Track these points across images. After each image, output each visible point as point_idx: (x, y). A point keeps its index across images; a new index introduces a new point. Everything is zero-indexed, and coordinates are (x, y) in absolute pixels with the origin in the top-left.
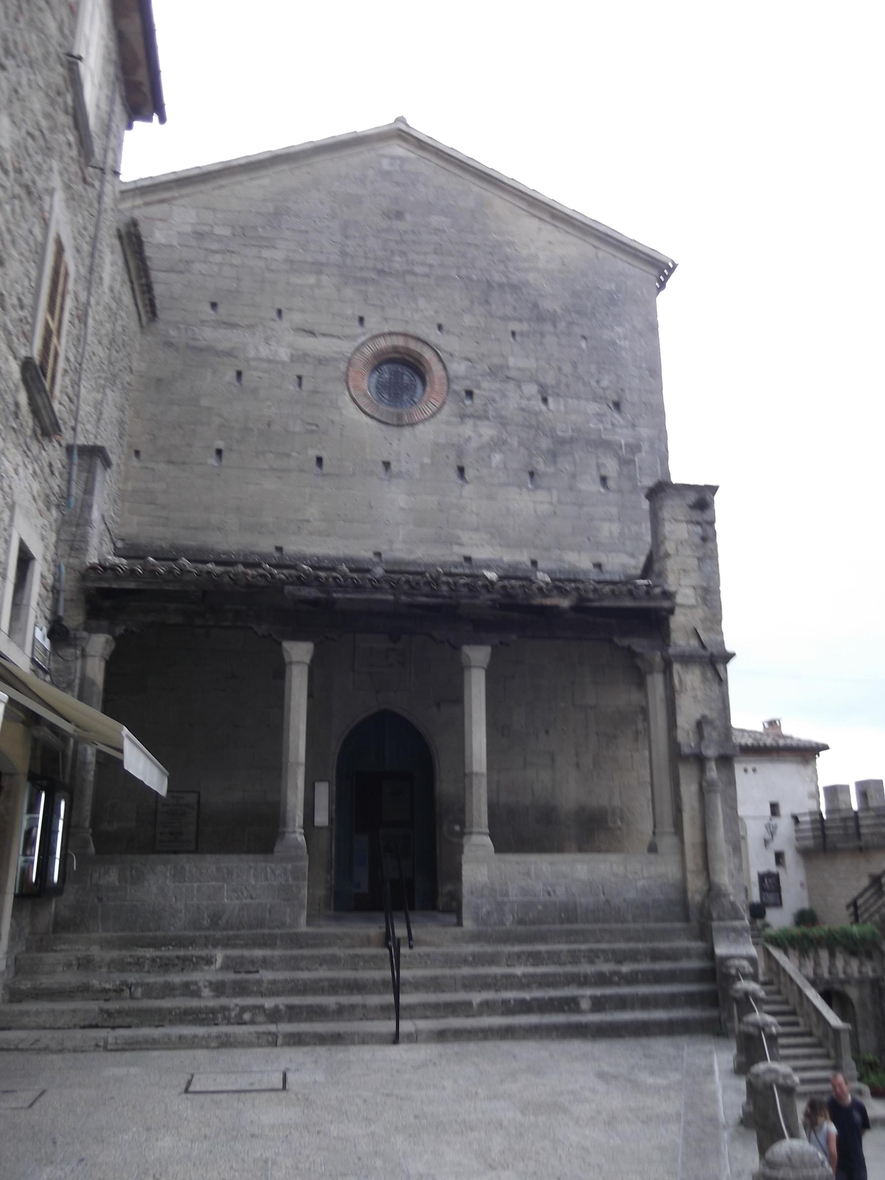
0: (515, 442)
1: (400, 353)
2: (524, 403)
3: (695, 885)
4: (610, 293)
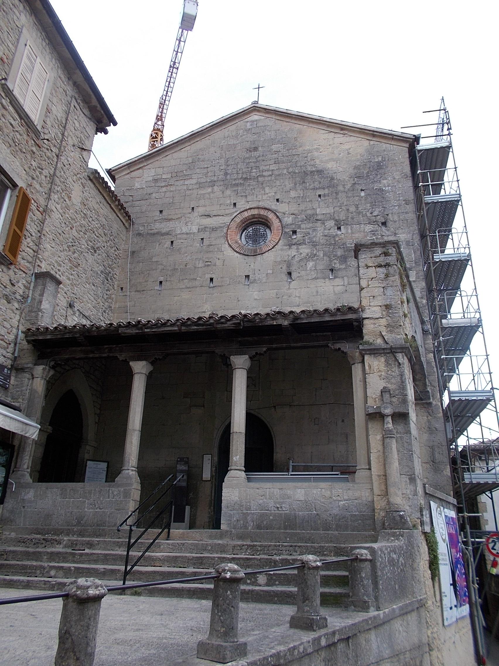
0: (321, 254)
1: (256, 218)
2: (326, 232)
3: (380, 504)
4: (379, 163)
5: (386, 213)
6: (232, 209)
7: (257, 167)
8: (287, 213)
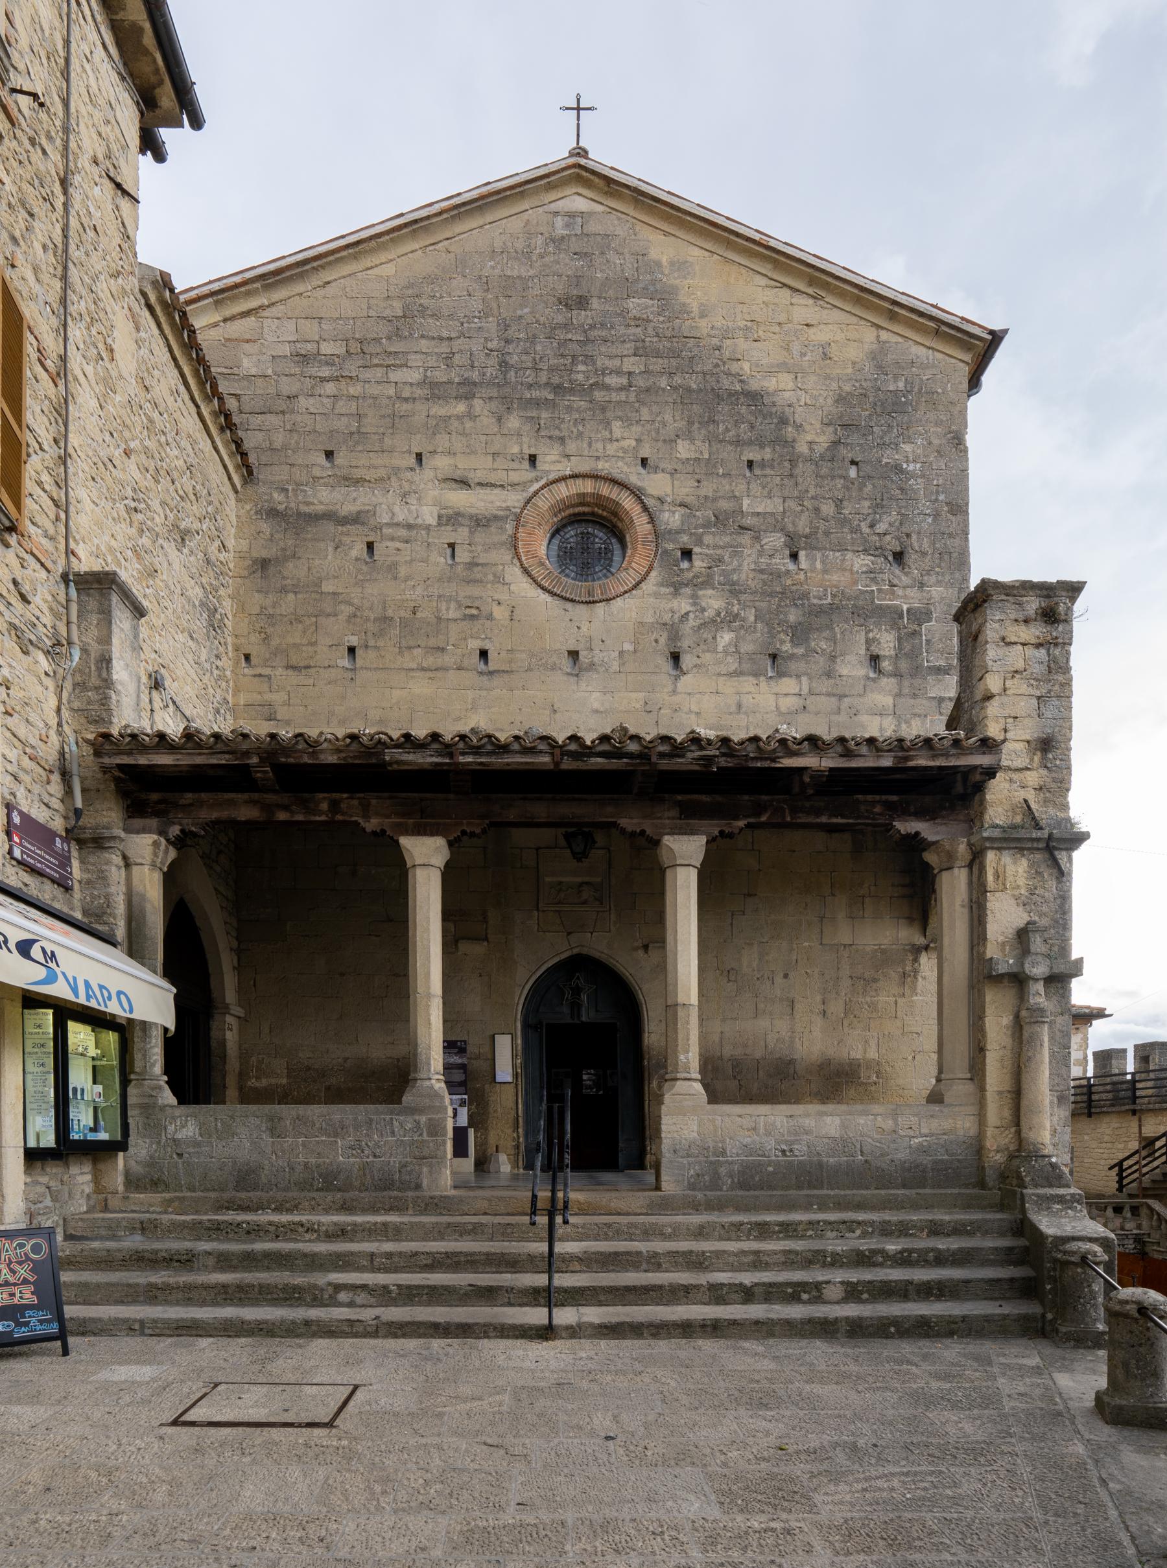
5: (904, 530)
6: (524, 473)
7: (589, 359)
8: (669, 499)
